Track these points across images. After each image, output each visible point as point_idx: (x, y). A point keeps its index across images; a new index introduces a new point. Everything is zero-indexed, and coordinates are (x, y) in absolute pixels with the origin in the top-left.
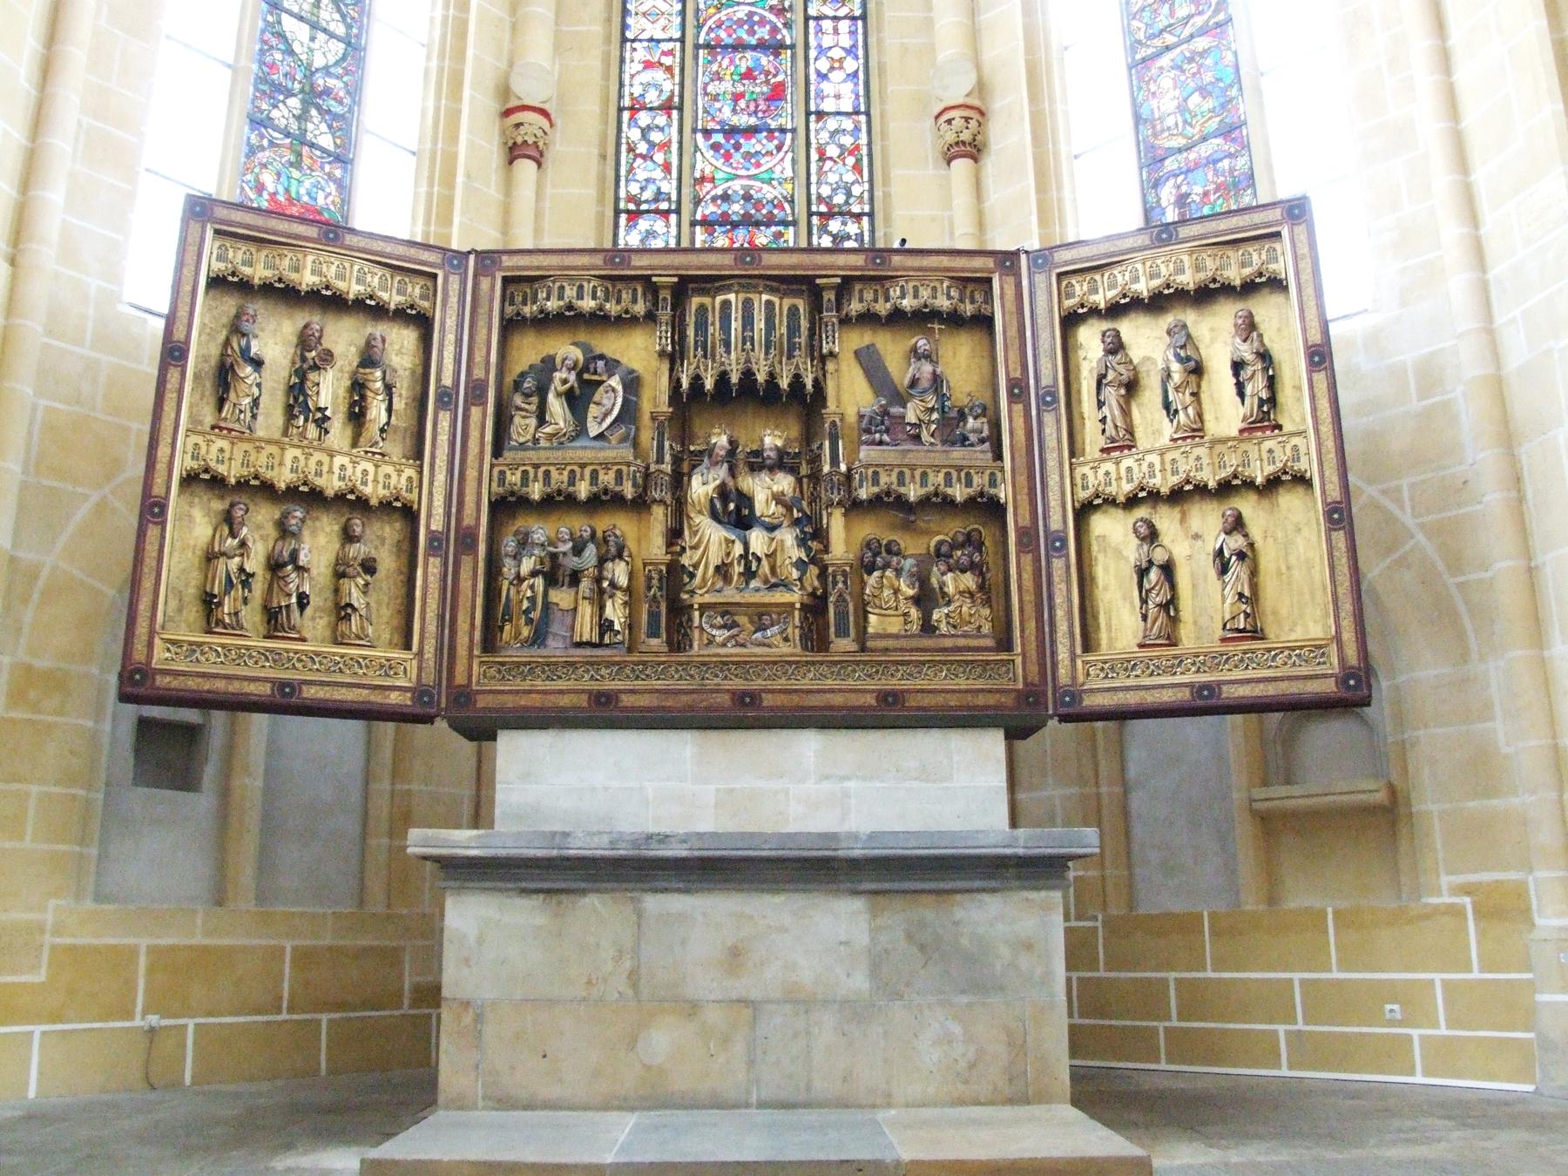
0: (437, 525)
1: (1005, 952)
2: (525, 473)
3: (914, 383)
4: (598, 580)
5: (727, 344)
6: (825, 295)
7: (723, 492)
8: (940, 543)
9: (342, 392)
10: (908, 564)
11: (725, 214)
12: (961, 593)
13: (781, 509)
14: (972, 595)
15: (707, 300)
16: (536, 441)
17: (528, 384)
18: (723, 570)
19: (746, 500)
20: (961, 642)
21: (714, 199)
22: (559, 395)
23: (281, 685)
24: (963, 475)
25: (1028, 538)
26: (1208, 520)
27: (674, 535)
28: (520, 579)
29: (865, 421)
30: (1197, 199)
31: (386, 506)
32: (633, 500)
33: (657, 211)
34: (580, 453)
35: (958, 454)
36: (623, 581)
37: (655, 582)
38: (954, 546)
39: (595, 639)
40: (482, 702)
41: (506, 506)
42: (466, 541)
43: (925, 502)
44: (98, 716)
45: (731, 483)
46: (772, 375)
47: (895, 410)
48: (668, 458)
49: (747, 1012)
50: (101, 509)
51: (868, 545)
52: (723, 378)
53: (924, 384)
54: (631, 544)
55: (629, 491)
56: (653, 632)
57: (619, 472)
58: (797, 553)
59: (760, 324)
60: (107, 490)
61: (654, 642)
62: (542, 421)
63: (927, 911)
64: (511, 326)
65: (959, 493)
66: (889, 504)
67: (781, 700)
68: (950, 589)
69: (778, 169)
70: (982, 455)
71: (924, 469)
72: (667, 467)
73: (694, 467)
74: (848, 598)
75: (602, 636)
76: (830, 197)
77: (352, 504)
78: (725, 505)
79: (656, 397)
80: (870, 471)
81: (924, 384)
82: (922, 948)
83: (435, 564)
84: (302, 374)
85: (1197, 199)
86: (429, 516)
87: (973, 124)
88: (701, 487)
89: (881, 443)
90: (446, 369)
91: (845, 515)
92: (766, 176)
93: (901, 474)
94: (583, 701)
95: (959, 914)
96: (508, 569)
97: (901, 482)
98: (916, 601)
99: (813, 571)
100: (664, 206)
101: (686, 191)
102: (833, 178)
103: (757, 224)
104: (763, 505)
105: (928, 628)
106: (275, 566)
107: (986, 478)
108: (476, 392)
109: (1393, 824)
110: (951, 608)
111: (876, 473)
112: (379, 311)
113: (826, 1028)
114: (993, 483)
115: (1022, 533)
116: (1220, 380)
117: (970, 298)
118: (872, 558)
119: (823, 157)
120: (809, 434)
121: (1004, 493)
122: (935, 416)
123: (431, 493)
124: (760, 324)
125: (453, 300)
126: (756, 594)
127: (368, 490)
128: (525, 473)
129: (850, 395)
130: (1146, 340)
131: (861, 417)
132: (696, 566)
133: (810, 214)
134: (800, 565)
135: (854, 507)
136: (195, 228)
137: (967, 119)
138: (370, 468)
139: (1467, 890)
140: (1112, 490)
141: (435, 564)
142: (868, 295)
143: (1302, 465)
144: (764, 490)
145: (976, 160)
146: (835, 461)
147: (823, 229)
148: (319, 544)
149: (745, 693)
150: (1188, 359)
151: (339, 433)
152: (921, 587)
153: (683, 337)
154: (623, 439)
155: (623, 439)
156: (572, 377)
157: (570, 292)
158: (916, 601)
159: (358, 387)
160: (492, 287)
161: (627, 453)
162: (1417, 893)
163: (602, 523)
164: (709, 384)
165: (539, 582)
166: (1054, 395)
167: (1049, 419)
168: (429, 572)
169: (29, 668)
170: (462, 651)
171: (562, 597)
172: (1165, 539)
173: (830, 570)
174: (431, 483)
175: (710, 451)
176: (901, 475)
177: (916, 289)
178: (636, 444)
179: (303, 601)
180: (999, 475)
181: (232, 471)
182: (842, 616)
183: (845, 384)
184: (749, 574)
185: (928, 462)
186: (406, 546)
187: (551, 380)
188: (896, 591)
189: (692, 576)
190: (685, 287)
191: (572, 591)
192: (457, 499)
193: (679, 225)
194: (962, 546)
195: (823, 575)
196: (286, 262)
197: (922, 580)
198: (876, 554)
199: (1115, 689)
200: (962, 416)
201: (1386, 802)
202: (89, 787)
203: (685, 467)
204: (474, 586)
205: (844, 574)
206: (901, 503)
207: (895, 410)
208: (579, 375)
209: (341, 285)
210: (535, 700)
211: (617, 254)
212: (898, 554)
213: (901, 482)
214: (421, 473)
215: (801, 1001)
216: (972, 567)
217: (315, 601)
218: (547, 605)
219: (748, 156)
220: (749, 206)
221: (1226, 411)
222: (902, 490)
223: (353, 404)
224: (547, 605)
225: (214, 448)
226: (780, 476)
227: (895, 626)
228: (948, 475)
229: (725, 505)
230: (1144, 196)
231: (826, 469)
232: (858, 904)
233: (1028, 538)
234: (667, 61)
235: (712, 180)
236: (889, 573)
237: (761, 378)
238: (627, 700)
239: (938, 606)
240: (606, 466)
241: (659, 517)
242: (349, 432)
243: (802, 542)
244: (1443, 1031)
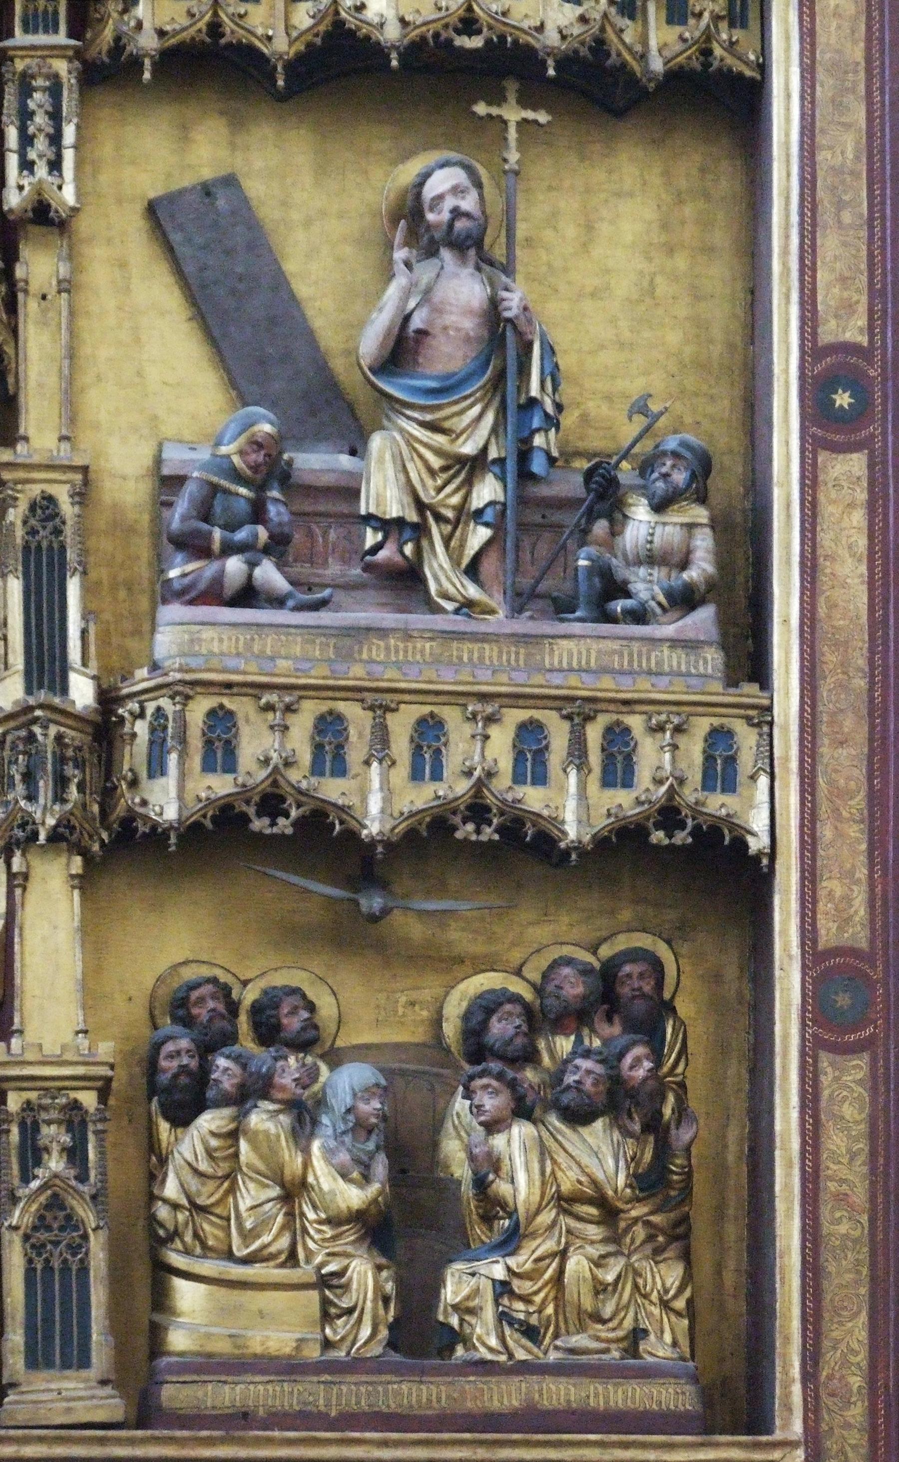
8: (486, 1006)
10: (346, 1083)
12: (565, 1202)
14: (609, 1213)
20: (558, 1393)
24: (594, 734)
29: (182, 505)
38: (540, 1018)
47: (315, 462)
51: (180, 1007)
66: (269, 840)
68: (521, 1186)
74: (88, 1216)
80: (199, 709)
91: (84, 883)
98: (376, 1229)
105: (420, 1334)
107: (694, 749)
110: (521, 1261)
111: (220, 718)
114: (721, 770)
118: (192, 1059)
121: (762, 812)
131: (169, 484)
135: (122, 854)
152: (399, 1175)
158: (376, 1229)
173: (14, 1102)
176: (330, 727)
180: (747, 739)
183: (101, 349)
185: (448, 680)
188: (293, 1191)
194: (577, 1017)
197: (403, 1146)
205: (74, 1119)
212: (304, 1043)
216: (614, 1101)
227: (280, 1325)
236: (262, 1119)
239: (461, 1247)
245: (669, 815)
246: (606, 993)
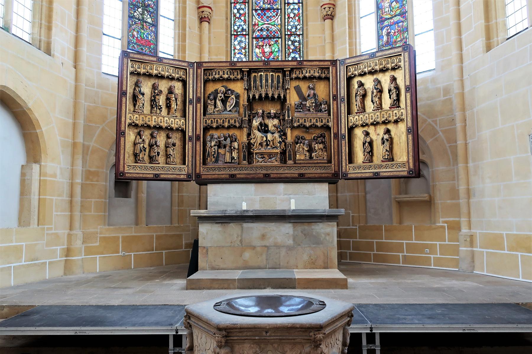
0: (190, 134)
1: (323, 235)
2: (212, 121)
3: (309, 96)
4: (231, 147)
5: (261, 86)
6: (285, 72)
7: (261, 124)
9: (164, 100)
11: (261, 35)
13: (275, 128)
15: (256, 74)
16: (214, 112)
17: (212, 97)
18: (261, 144)
19: (266, 126)
21: (258, 31)
22: (219, 100)
23: (156, 175)
25: (336, 135)
26: (381, 129)
27: (249, 135)
28: (211, 147)
30: (392, 34)
31: (177, 129)
32: (239, 127)
33: (242, 35)
34: (225, 115)
35: (319, 114)
36: (237, 147)
37: (245, 147)
38: (318, 137)
39: (230, 161)
40: (203, 177)
41: (206, 129)
42: (198, 138)
43: (311, 126)
44: (106, 182)
45: (263, 122)
46: (273, 94)
47: (303, 103)
48: (247, 116)
49: (266, 249)
50: (103, 130)
52: (260, 95)
53: (311, 96)
54: (238, 137)
55: (237, 125)
56: (245, 160)
57: (235, 120)
58: (279, 140)
59: (270, 81)
60: (104, 125)
61: (245, 162)
62: (215, 107)
63: (306, 227)
64: (206, 82)
65: (319, 124)
66: (301, 127)
67: (275, 175)
69: (276, 21)
70: (325, 114)
71: (311, 118)
72: (247, 118)
73: (254, 117)
75: (232, 160)
76: (291, 29)
77: (169, 129)
78: (261, 128)
79: (243, 101)
81: (311, 96)
82: (305, 235)
83: (190, 143)
84: (154, 96)
85: (392, 34)
86: (188, 131)
87: (331, 9)
88: (256, 123)
89: (300, 112)
90: (190, 95)
92: (273, 23)
93: (305, 120)
94: (228, 176)
95: (313, 227)
96: (208, 144)
97: (305, 122)
99: (283, 144)
100: (244, 33)
101: (250, 29)
102: (292, 24)
103: (271, 38)
104: (271, 128)
106: (151, 146)
108: (198, 100)
109: (430, 206)
112: (173, 79)
113: (283, 252)
114: (328, 122)
115: (334, 134)
116: (386, 95)
117: (325, 71)
118: (298, 140)
119: (289, 18)
120: (282, 109)
121: (330, 124)
122: (314, 104)
123: (188, 126)
124: (270, 81)
125: (191, 76)
126: (269, 150)
127: (173, 126)
128: (212, 121)
129: (293, 99)
130: (369, 82)
132: (254, 143)
133: (285, 35)
134: (280, 142)
136: (125, 60)
137: (330, 8)
138: (173, 120)
139: (446, 222)
140: (357, 123)
141: (190, 143)
142: (298, 73)
143: (403, 117)
144: (272, 123)
145: (332, 20)
146: (289, 117)
147: (289, 39)
148: (161, 139)
149: (266, 174)
150: (378, 89)
151: (164, 111)
153: (250, 84)
154: (236, 111)
155: (236, 111)
156: (223, 96)
157: (221, 73)
159: (168, 99)
160: (201, 71)
161: (236, 115)
162: (435, 223)
163: (231, 132)
164: (257, 97)
165: (216, 147)
166: (344, 99)
167: (342, 105)
168: (189, 146)
169: (89, 171)
170: (198, 165)
171: (222, 151)
172: (371, 135)
174: (189, 124)
175: (257, 113)
177: (310, 71)
178: (239, 112)
179: (158, 154)
181: (140, 123)
182: (290, 155)
183: (291, 96)
184: (267, 145)
186: (182, 139)
187: (217, 96)
189: (253, 145)
190: (250, 72)
191: (224, 150)
192: (195, 128)
193: (249, 39)
194: (320, 137)
195: (285, 145)
196: (149, 67)
198: (299, 139)
199: (356, 173)
200: (321, 104)
201: (428, 200)
202: (105, 199)
203: (252, 117)
204: (200, 149)
206: (305, 127)
207: (303, 103)
208: (224, 95)
209: (163, 73)
210: (216, 176)
211: (232, 63)
213: (305, 122)
214: (186, 121)
215: (278, 246)
217: (161, 153)
218: (218, 153)
219: (268, 17)
220: (268, 33)
221: (387, 102)
222: (305, 124)
223: (167, 104)
224: (218, 153)
225: (135, 117)
226: (275, 120)
227: (303, 158)
228: (317, 120)
229: (261, 128)
230: (378, 32)
231: (286, 118)
232: (290, 225)
233: (336, 135)
235: (258, 25)
237: (270, 95)
238: (238, 176)
240: (232, 119)
241: (245, 131)
242: (167, 111)
243: (280, 137)
244: (439, 256)
245: (325, 124)
246: (321, 136)
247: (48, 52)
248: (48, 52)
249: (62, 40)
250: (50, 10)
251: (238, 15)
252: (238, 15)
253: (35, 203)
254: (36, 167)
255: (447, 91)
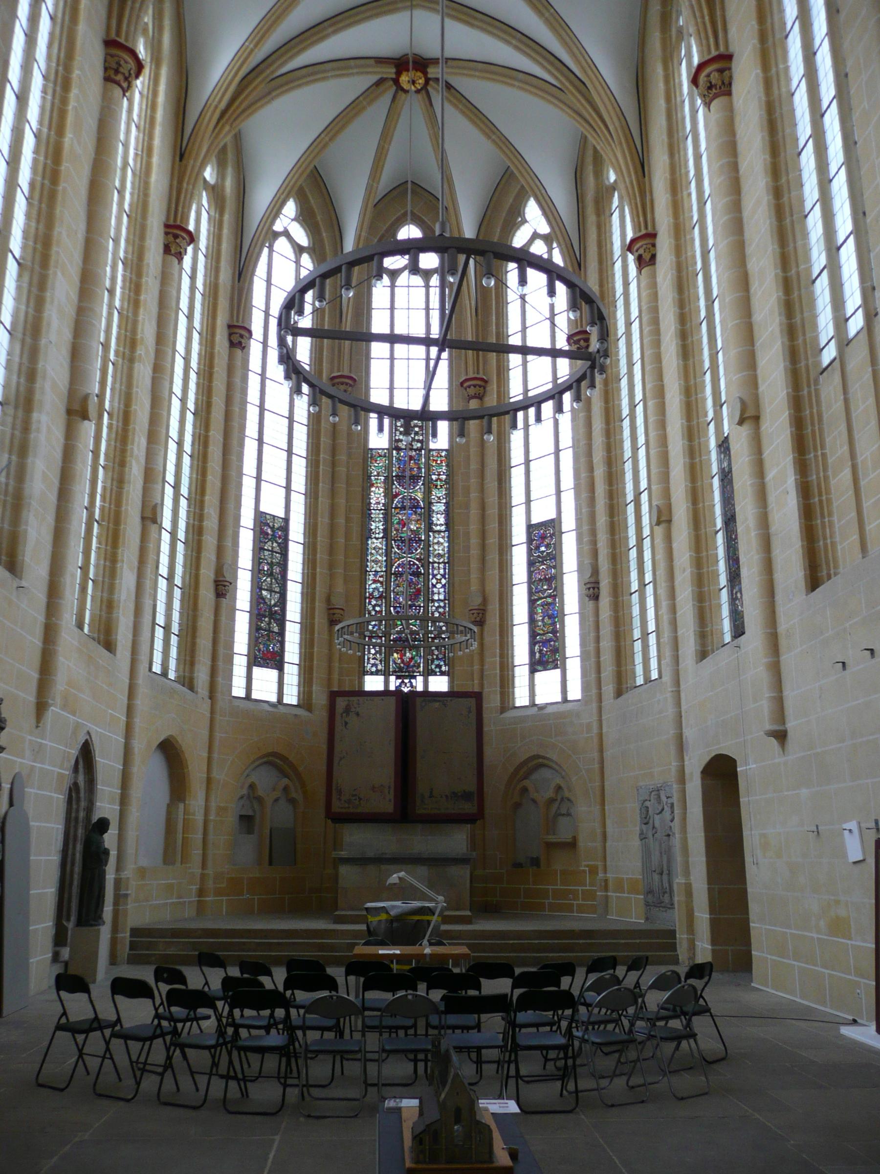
234: (381, 579)
247: (191, 688)
248: (191, 688)
249: (202, 676)
250: (194, 644)
251: (373, 613)
252: (373, 613)
253: (179, 842)
254: (181, 806)
255: (589, 726)
